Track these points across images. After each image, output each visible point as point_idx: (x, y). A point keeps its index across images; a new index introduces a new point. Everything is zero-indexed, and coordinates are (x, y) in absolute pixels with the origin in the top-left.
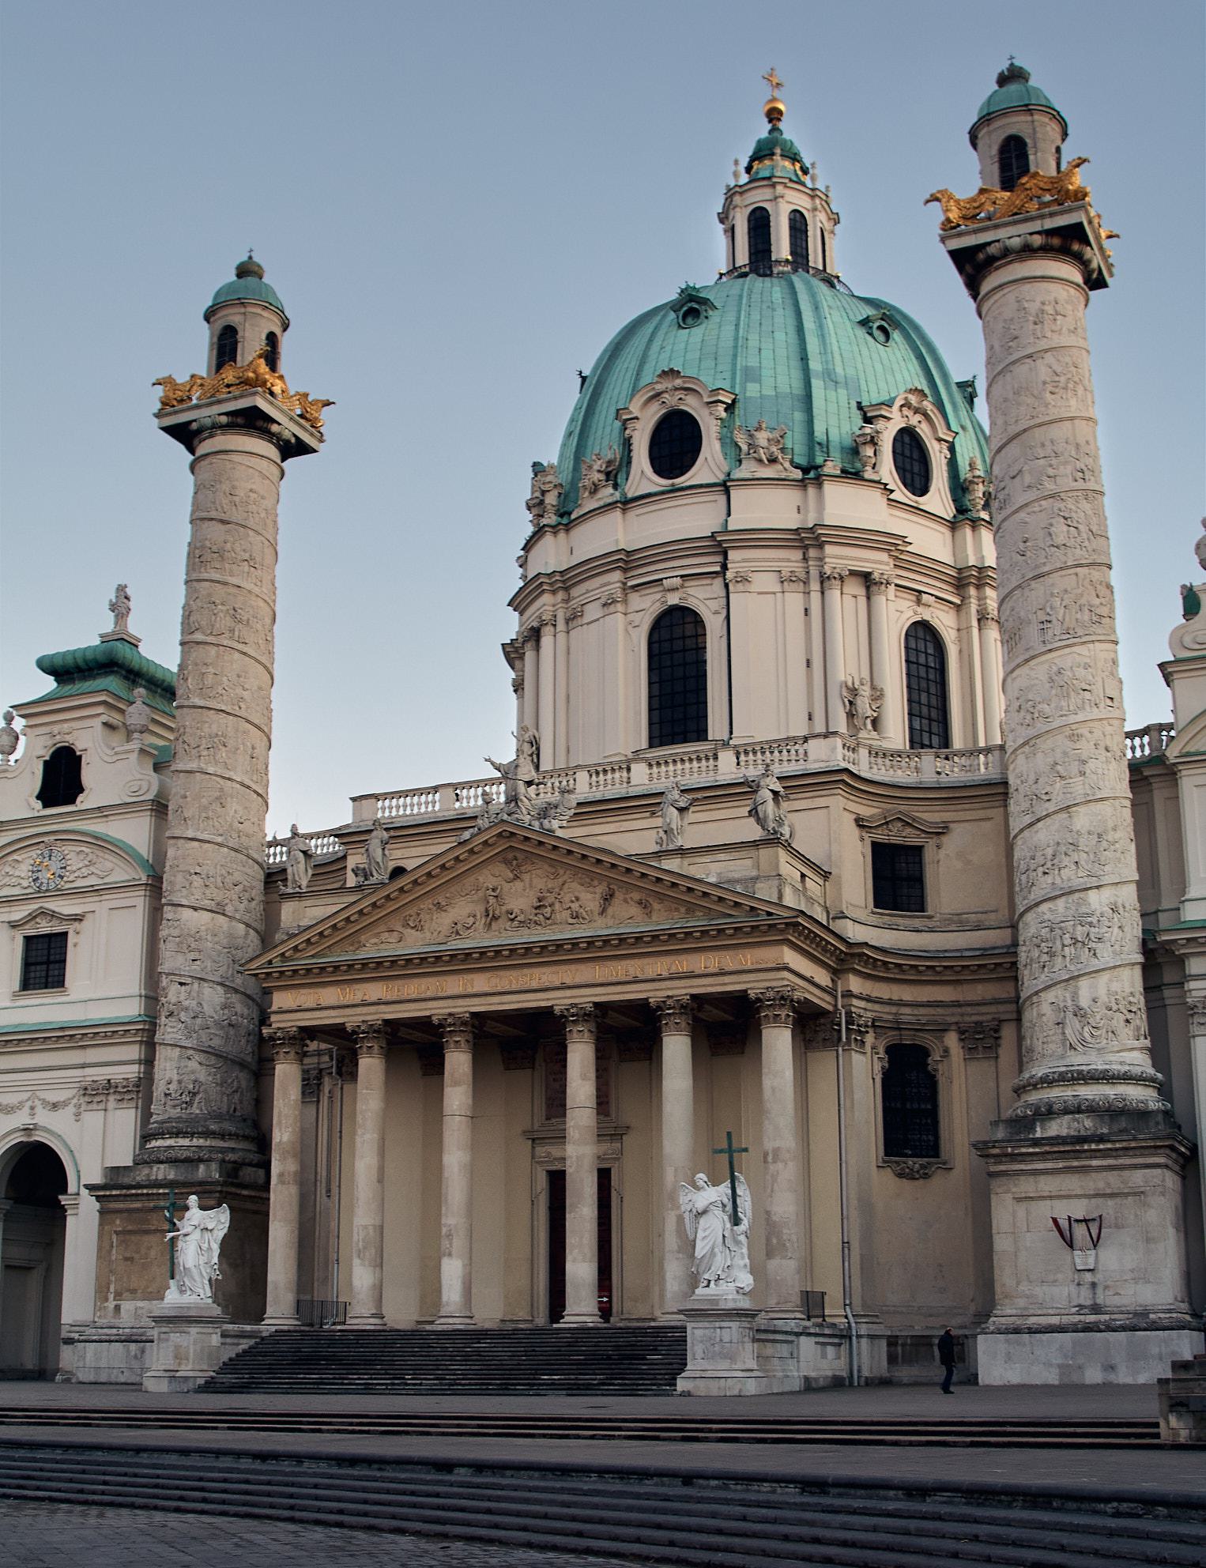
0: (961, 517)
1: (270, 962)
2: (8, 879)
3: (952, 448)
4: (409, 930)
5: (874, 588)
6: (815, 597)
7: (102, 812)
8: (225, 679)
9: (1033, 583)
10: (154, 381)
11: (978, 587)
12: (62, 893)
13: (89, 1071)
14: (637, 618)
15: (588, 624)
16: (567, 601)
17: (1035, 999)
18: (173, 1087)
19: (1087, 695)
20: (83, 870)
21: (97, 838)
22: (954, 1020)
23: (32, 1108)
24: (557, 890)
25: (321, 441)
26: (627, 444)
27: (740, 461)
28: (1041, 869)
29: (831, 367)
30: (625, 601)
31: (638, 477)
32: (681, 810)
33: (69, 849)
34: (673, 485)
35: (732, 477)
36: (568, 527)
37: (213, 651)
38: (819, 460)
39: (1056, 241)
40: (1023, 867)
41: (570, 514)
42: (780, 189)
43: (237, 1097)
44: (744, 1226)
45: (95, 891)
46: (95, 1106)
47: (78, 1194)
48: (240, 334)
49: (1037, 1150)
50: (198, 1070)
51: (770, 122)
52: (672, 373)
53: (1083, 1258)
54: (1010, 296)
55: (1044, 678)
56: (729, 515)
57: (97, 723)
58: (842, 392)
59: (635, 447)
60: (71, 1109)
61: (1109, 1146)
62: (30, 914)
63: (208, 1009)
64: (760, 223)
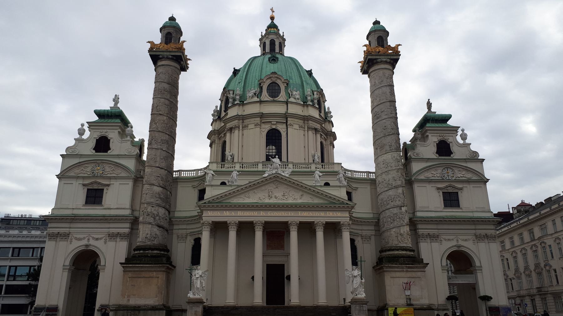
1: (205, 203)
2: (82, 171)
4: (246, 198)
5: (317, 132)
7: (118, 156)
8: (168, 125)
9: (387, 137)
10: (148, 41)
11: (330, 136)
13: (111, 230)
14: (263, 130)
15: (250, 129)
16: (243, 122)
17: (389, 230)
18: (148, 236)
19: (399, 162)
20: (111, 172)
21: (116, 163)
22: (361, 233)
23: (88, 239)
24: (288, 192)
25: (188, 69)
26: (261, 88)
27: (290, 98)
28: (390, 201)
29: (306, 80)
30: (260, 125)
31: (264, 96)
32: (320, 176)
34: (274, 100)
35: (289, 100)
37: (165, 118)
38: (306, 101)
39: (392, 61)
40: (384, 200)
41: (243, 102)
42: (278, 36)
43: (166, 239)
44: (363, 281)
45: (115, 178)
46: (112, 240)
47: (105, 266)
48: (173, 35)
49: (396, 266)
53: (408, 293)
54: (381, 72)
55: (390, 157)
56: (287, 109)
57: (116, 131)
58: (309, 86)
60: (103, 240)
61: (413, 266)
62: (91, 182)
63: (160, 215)
64: (272, 43)
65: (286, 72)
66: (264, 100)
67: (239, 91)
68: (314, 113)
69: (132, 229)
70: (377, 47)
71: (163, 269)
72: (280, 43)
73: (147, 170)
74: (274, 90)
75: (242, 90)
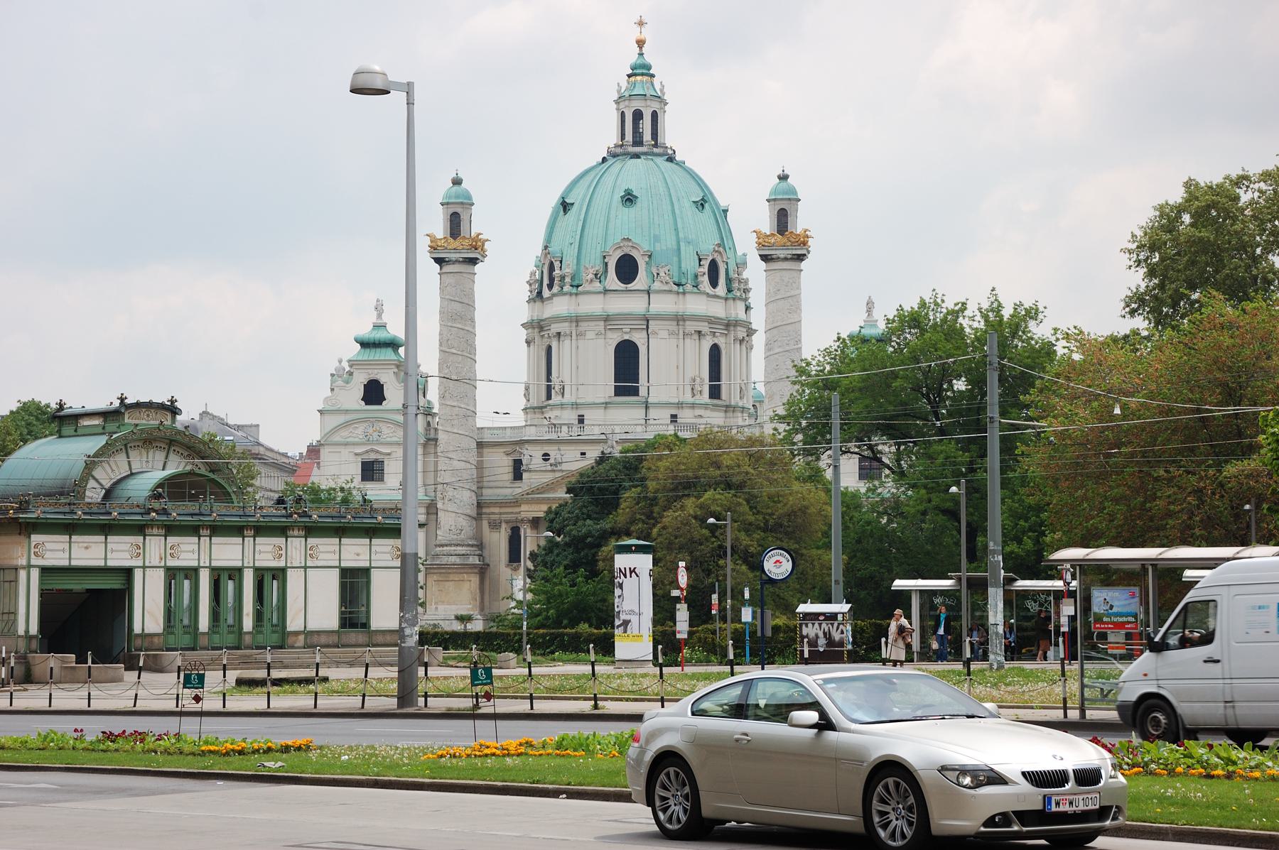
0: (730, 295)
3: (727, 264)
6: (682, 341)
12: (382, 444)
16: (577, 326)
26: (606, 264)
33: (381, 424)
35: (652, 288)
36: (576, 294)
41: (578, 286)
50: (463, 522)
51: (641, 48)
52: (628, 240)
57: (391, 372)
58: (691, 247)
59: (609, 267)
63: (465, 499)
64: (638, 115)
65: (650, 228)
66: (610, 288)
67: (567, 270)
68: (696, 305)
69: (428, 514)
70: (773, 235)
71: (476, 571)
72: (655, 116)
73: (441, 436)
74: (627, 268)
75: (575, 261)
